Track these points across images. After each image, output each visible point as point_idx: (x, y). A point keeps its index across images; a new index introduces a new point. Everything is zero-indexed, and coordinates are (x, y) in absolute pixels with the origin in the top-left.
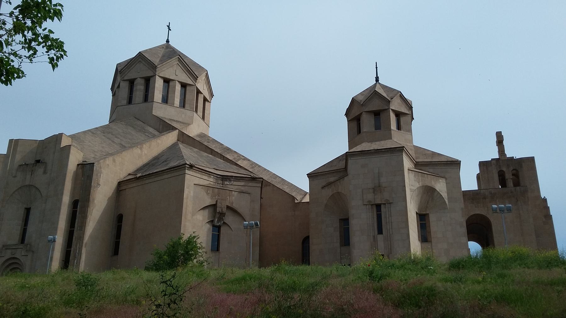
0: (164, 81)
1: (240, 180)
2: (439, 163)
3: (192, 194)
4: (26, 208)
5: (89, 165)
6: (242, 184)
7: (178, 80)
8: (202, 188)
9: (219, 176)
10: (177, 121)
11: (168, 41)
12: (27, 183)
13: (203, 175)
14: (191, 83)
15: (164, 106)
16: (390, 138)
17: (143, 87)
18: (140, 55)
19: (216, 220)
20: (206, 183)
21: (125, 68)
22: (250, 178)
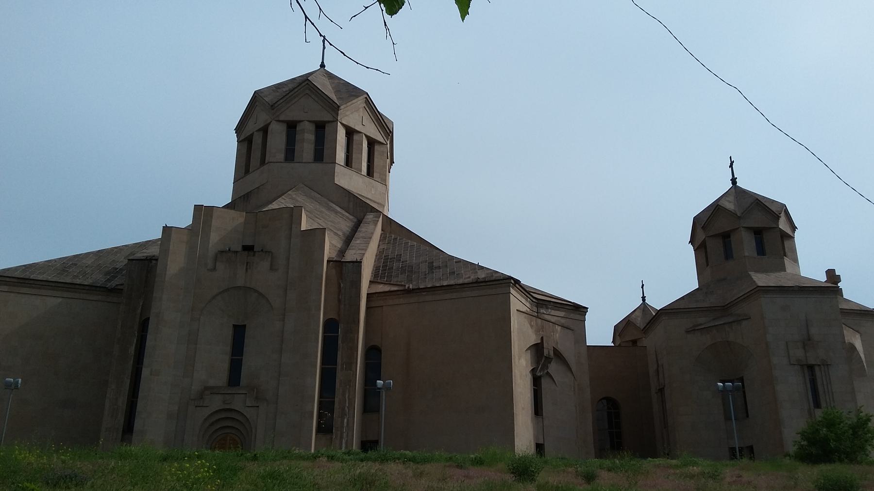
0: (346, 133)
1: (560, 309)
2: (852, 311)
3: (516, 326)
4: (233, 325)
5: (352, 264)
6: (562, 314)
7: (365, 133)
8: (525, 317)
9: (534, 300)
10: (367, 198)
11: (323, 66)
12: (240, 283)
13: (522, 296)
14: (382, 140)
15: (347, 171)
16: (783, 268)
17: (314, 136)
18: (307, 84)
19: (540, 367)
20: (524, 309)
21: (281, 101)
22: (572, 307)
